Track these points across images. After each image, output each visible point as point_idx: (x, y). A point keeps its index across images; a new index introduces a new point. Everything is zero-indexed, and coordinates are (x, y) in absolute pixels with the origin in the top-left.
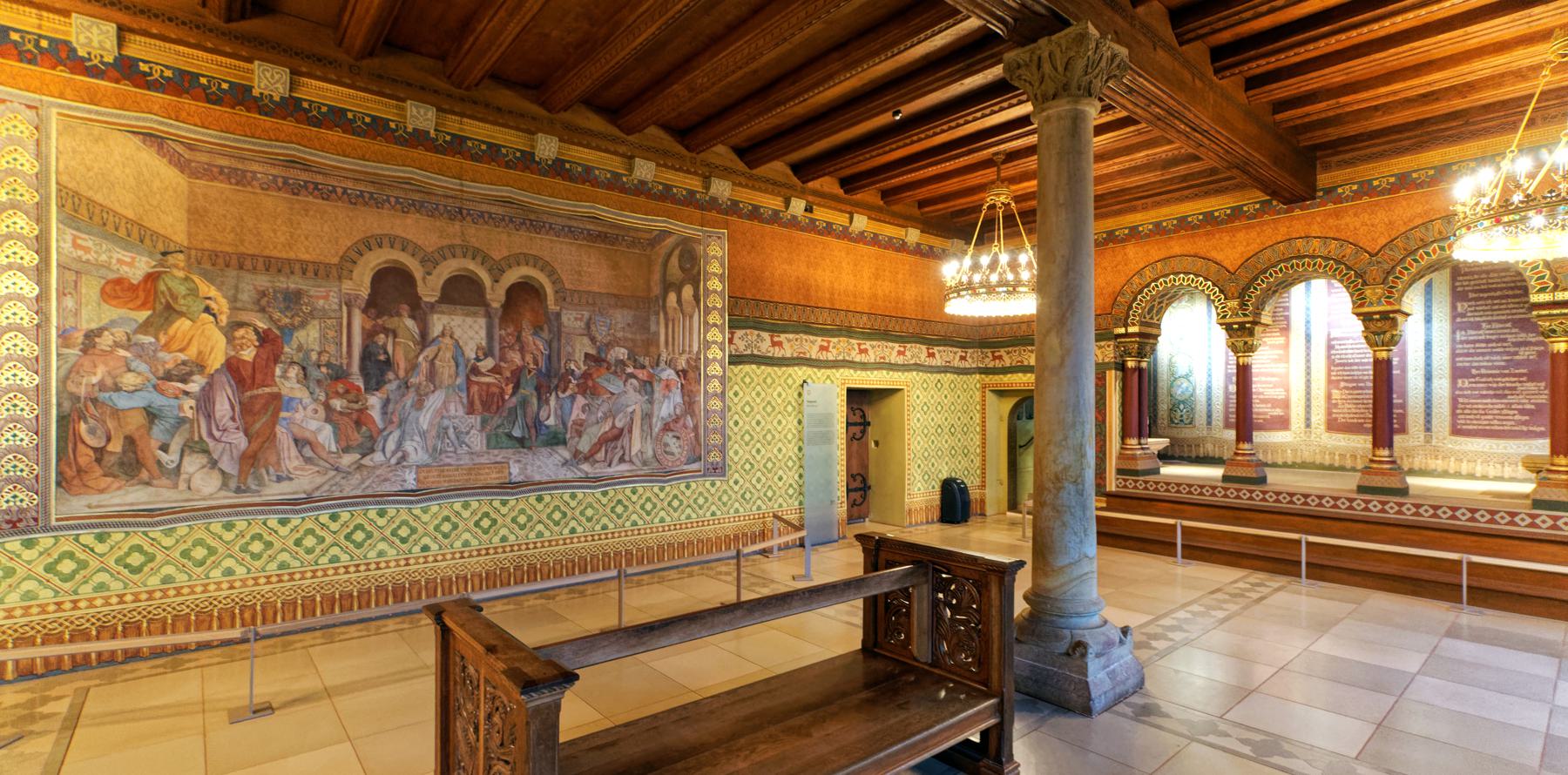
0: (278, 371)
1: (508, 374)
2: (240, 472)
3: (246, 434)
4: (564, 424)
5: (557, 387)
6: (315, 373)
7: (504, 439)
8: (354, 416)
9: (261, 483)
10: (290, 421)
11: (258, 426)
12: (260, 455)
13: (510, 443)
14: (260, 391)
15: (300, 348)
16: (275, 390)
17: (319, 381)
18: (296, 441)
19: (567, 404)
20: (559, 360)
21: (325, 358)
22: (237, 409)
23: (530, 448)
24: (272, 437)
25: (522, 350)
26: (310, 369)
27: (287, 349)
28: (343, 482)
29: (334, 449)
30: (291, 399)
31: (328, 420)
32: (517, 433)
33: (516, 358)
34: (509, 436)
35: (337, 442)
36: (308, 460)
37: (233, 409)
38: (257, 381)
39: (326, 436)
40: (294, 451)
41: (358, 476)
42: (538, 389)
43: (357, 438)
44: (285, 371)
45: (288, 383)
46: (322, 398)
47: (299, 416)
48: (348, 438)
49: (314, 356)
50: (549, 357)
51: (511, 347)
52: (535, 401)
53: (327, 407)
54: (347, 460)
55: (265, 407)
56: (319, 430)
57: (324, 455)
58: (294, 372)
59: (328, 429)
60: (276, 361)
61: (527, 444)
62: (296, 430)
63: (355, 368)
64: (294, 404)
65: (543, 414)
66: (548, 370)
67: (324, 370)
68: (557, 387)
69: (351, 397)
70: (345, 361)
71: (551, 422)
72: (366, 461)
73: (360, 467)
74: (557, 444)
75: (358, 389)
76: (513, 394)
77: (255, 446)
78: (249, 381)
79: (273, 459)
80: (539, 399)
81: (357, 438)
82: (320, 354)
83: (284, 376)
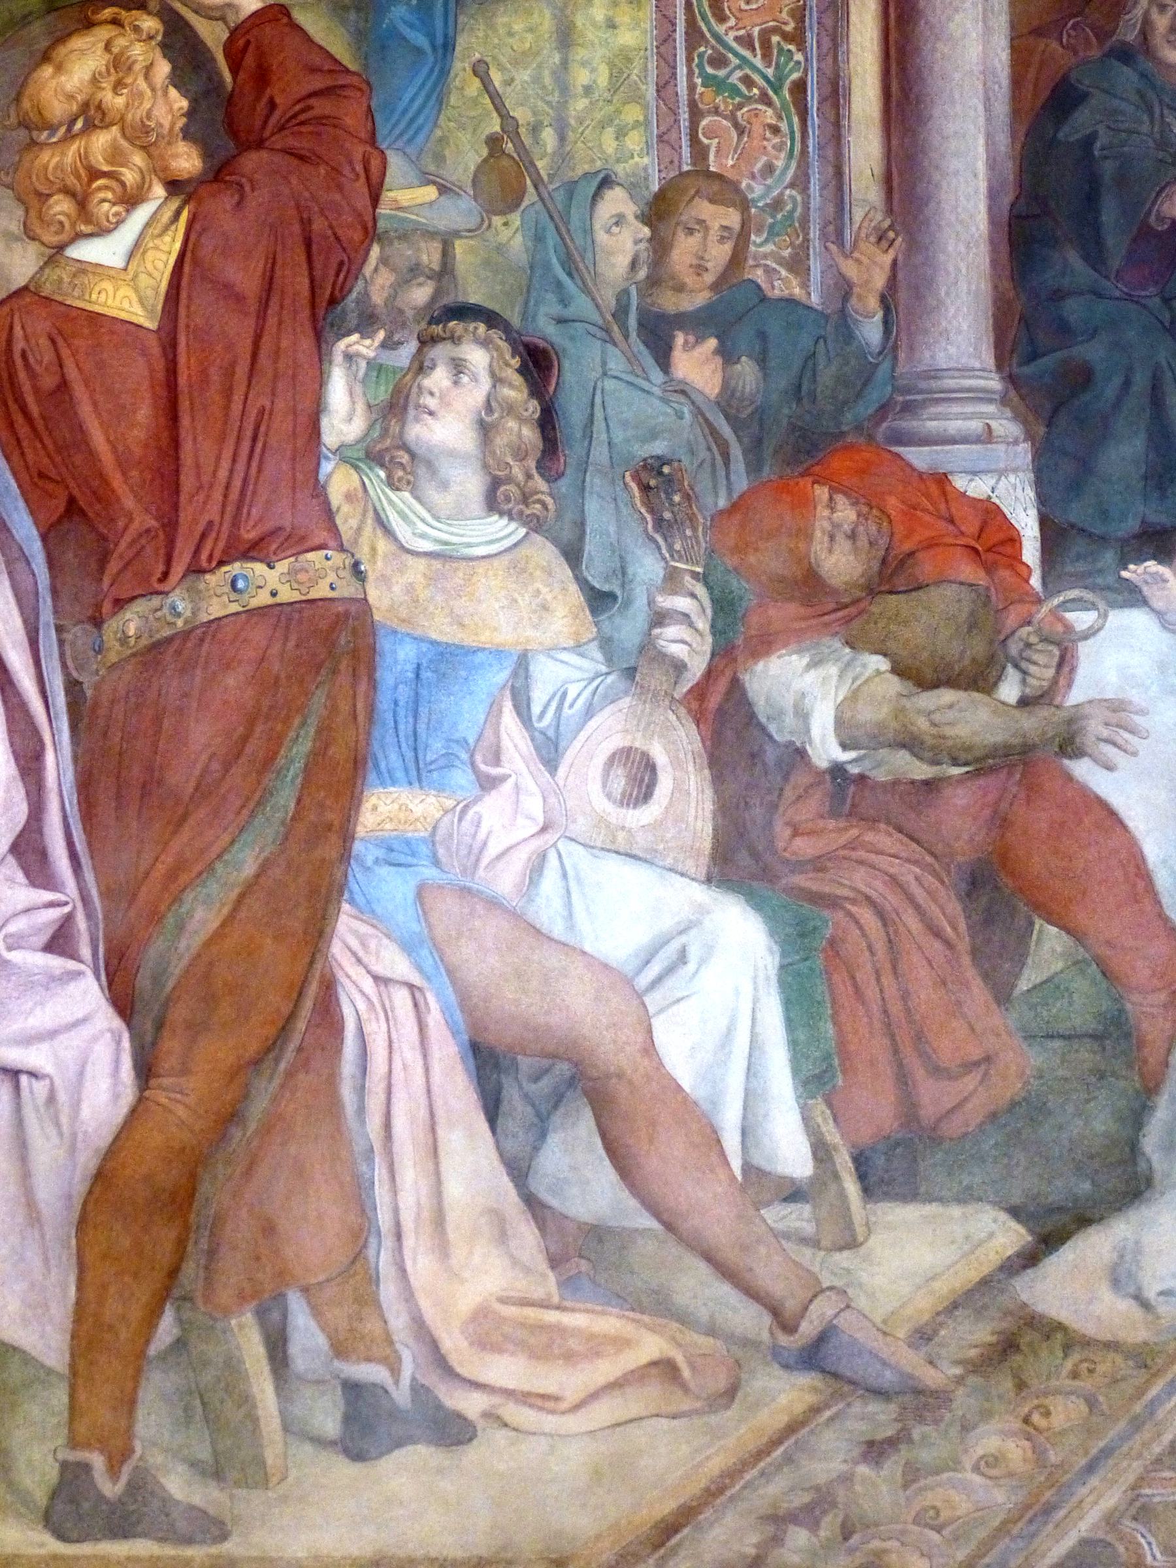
0: (344, 413)
2: (89, 1333)
3: (124, 1002)
6: (637, 405)
8: (961, 816)
9: (233, 1461)
10: (453, 886)
11: (202, 914)
12: (214, 1191)
14: (215, 597)
15: (506, 175)
16: (322, 575)
17: (655, 481)
18: (488, 1062)
21: (700, 250)
22: (58, 766)
24: (301, 1019)
26: (598, 372)
27: (406, 196)
28: (877, 1488)
29: (790, 1151)
30: (446, 661)
31: (736, 862)
35: (817, 1080)
36: (580, 1253)
37: (29, 764)
38: (197, 512)
39: (719, 1010)
40: (471, 1162)
41: (994, 1439)
43: (993, 1045)
44: (395, 405)
45: (428, 517)
46: (688, 644)
47: (503, 823)
48: (907, 1040)
49: (617, 240)
53: (727, 722)
54: (917, 1257)
55: (252, 746)
56: (671, 956)
57: (711, 1206)
58: (461, 400)
59: (740, 944)
60: (328, 309)
62: (483, 957)
63: (960, 332)
64: (467, 709)
67: (697, 365)
69: (935, 616)
70: (871, 271)
72: (1072, 1287)
73: (1019, 1344)
75: (992, 539)
77: (185, 1101)
78: (135, 512)
79: (313, 1240)
81: (993, 1045)
82: (659, 211)
83: (389, 451)
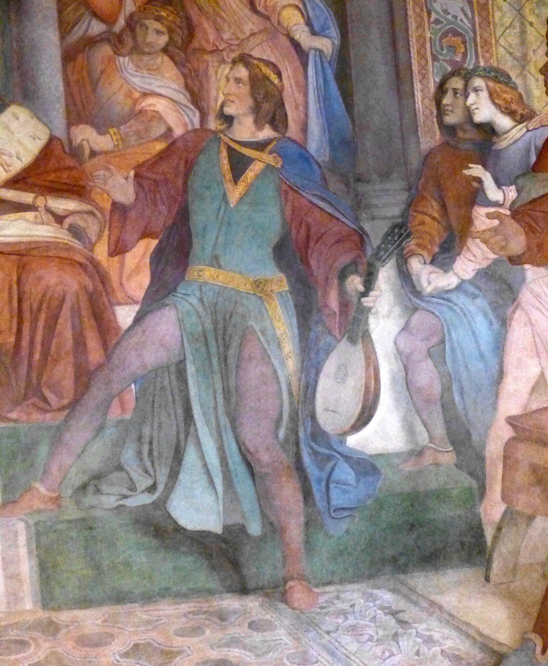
1: (120, 188)
4: (462, 440)
5: (400, 233)
7: (136, 554)
13: (168, 566)
19: (474, 322)
20: (401, 78)
23: (277, 592)
25: (184, 49)
32: (197, 508)
33: (154, 90)
34: (160, 530)
42: (293, 253)
50: (343, 69)
51: (125, 39)
52: (280, 322)
61: (263, 567)
65: (335, 395)
66: (344, 145)
68: (400, 232)
71: (385, 434)
74: (432, 559)
76: (161, 291)
80: (306, 310)
